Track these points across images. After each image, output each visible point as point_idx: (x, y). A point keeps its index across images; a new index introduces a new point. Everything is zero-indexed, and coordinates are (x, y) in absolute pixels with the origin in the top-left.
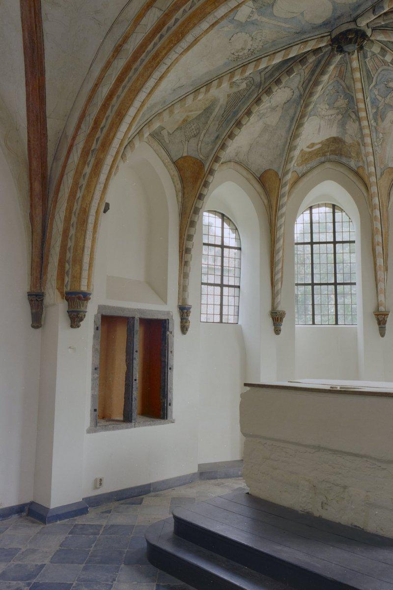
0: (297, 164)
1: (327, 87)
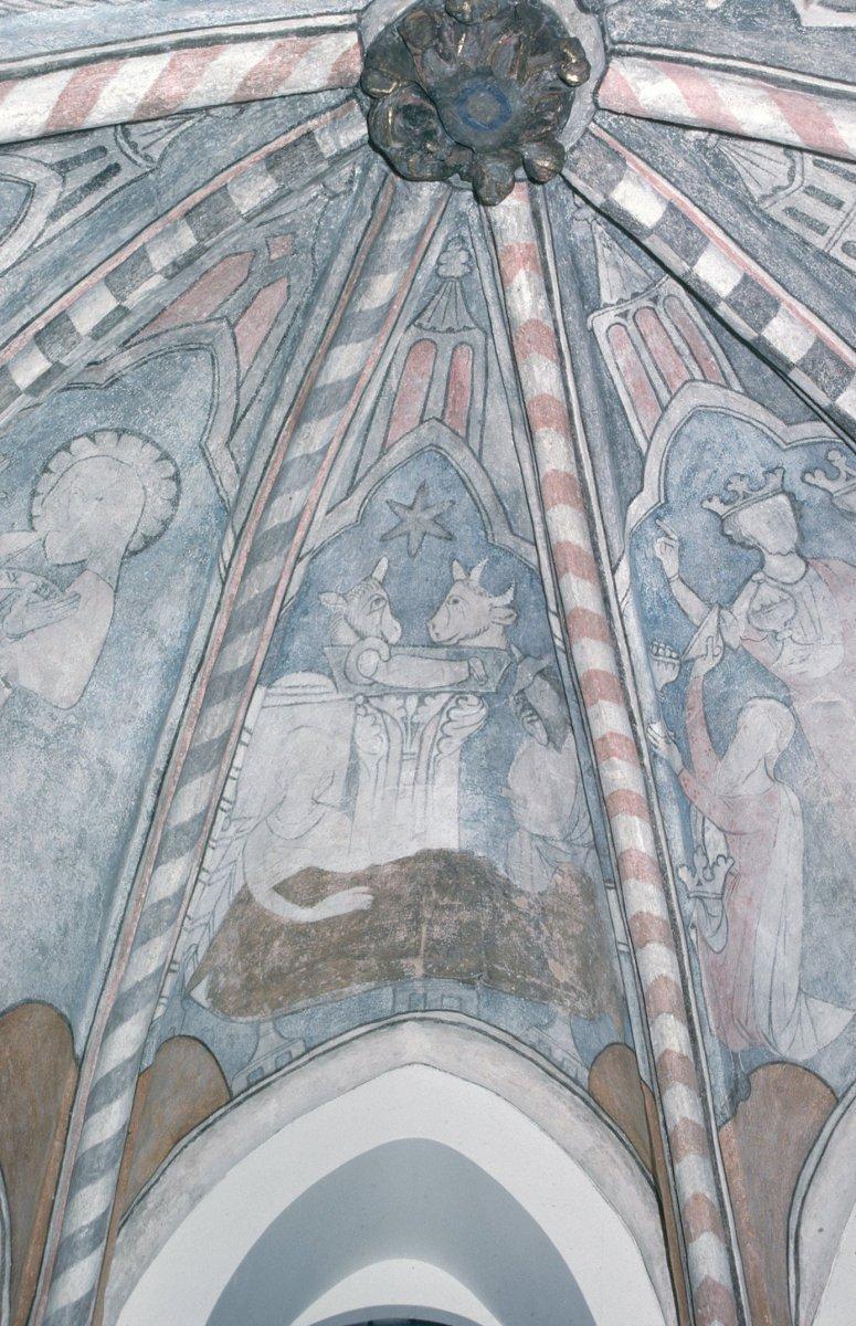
0: (211, 994)
1: (383, 480)
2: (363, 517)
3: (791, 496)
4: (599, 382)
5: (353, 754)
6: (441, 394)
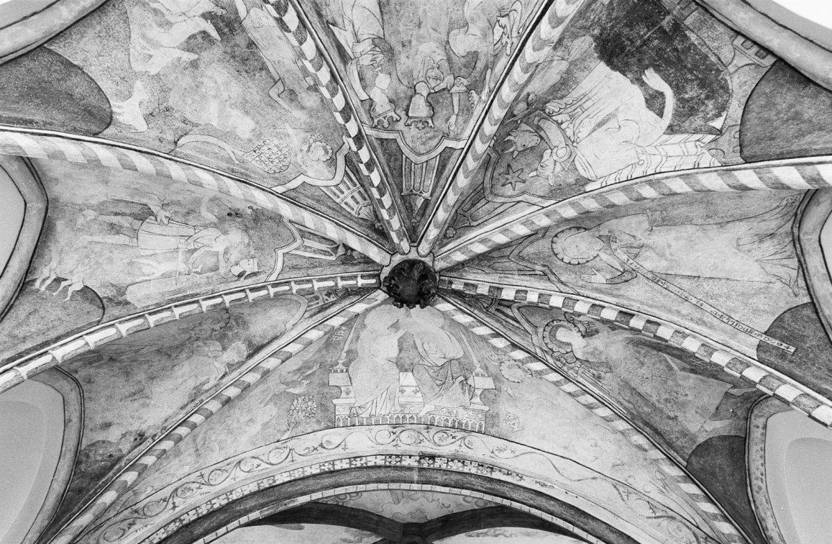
0: (718, 115)
1: (510, 197)
2: (523, 193)
3: (407, 115)
4: (438, 182)
5: (594, 130)
6: (479, 204)
